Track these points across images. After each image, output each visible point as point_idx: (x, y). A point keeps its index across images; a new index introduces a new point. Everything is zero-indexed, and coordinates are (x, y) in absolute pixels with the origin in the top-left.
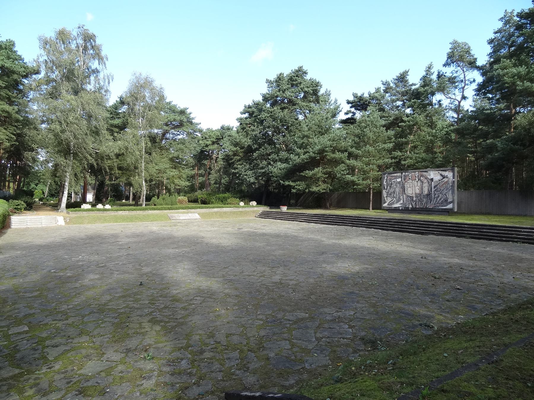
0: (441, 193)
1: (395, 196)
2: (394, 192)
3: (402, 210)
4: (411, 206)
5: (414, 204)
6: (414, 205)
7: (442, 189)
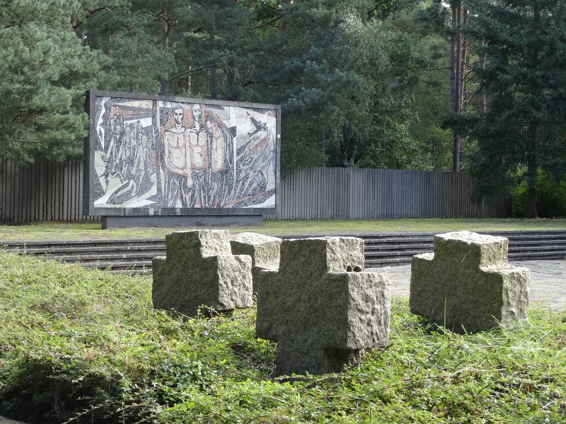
0: (252, 168)
1: (133, 172)
2: (131, 161)
3: (156, 216)
4: (179, 205)
5: (188, 197)
6: (188, 202)
7: (255, 157)
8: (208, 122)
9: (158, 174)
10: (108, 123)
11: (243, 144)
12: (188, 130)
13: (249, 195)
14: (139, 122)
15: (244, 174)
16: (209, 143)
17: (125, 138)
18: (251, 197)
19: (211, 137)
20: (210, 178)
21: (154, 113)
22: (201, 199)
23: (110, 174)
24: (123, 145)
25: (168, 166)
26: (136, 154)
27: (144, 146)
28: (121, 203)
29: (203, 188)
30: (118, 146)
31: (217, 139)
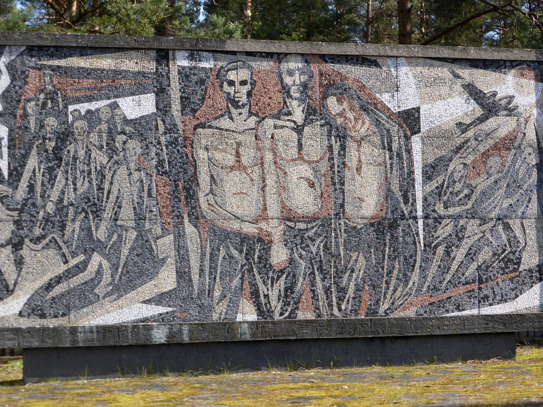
1: (101, 234)
6: (276, 305)
8: (332, 103)
9: (180, 236)
10: (19, 112)
11: (444, 153)
12: (270, 122)
13: (467, 283)
14: (115, 106)
15: (449, 229)
16: (336, 152)
17: (71, 148)
18: (475, 286)
19: (342, 137)
20: (341, 240)
21: (161, 84)
22: (315, 297)
23: (27, 240)
24: (67, 164)
25: (210, 215)
26: (106, 186)
27: (132, 166)
28: (64, 315)
29: (321, 269)
30: (50, 170)
31: (359, 142)
